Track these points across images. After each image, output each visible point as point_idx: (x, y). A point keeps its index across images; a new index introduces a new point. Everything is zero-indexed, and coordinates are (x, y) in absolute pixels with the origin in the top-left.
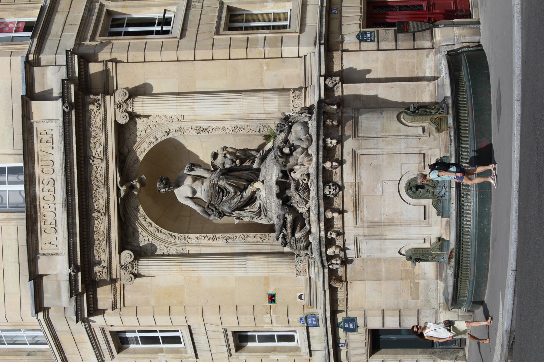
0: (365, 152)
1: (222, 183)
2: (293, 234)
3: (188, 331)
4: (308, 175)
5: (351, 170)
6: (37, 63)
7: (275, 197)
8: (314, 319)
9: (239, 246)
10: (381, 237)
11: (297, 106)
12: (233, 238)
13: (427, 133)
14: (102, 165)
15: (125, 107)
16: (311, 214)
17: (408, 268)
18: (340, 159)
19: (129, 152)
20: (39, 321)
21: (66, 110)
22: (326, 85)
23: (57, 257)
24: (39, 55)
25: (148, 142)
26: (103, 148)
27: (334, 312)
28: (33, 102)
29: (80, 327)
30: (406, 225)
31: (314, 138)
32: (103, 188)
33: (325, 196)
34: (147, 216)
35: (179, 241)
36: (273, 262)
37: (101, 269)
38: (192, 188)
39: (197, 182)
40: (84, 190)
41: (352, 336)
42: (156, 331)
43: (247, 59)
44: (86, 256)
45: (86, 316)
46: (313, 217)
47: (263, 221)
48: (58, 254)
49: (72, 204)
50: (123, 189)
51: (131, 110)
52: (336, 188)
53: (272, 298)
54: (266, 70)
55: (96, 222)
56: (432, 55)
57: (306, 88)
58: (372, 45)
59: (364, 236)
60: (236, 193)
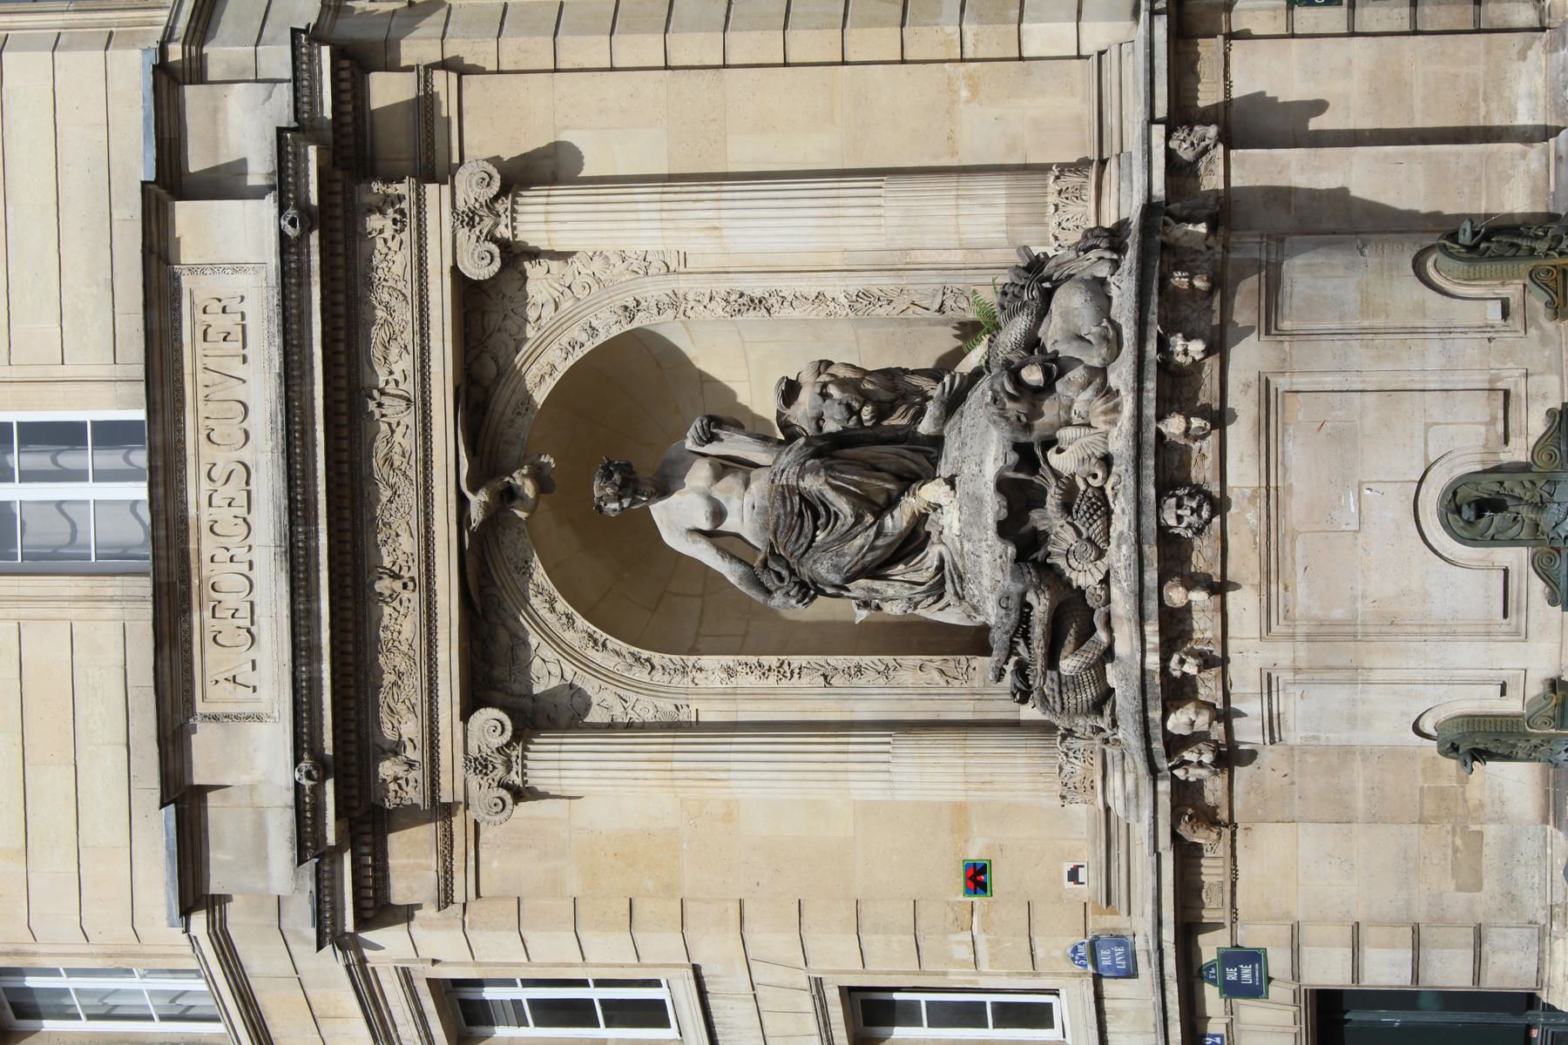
0: (1301, 382)
1: (813, 484)
2: (1052, 661)
3: (693, 983)
4: (1107, 461)
5: (1252, 444)
6: (196, 72)
7: (991, 533)
8: (1119, 951)
9: (867, 697)
10: (1354, 675)
11: (1070, 225)
12: (847, 672)
13: (1516, 321)
14: (409, 418)
15: (488, 222)
16: (1115, 592)
17: (1445, 783)
18: (1216, 406)
19: (500, 375)
20: (193, 940)
21: (291, 232)
22: (1170, 154)
23: (255, 726)
24: (201, 44)
25: (564, 341)
26: (412, 359)
27: (1189, 928)
28: (178, 203)
29: (331, 963)
30: (1441, 634)
31: (1128, 333)
32: (410, 496)
33: (1163, 531)
34: (557, 594)
35: (667, 678)
36: (983, 756)
37: (400, 770)
38: (710, 499)
39: (730, 481)
40: (346, 502)
41: (1249, 1010)
42: (583, 983)
43: (903, 61)
44: (352, 726)
45: (349, 926)
46: (1122, 605)
47: (953, 616)
48: (259, 718)
49: (306, 549)
50: (478, 502)
51: (507, 234)
52: (1200, 506)
53: (977, 878)
54: (968, 101)
55: (387, 610)
56: (1537, 53)
57: (1103, 163)
59: (1297, 670)
60: (859, 519)
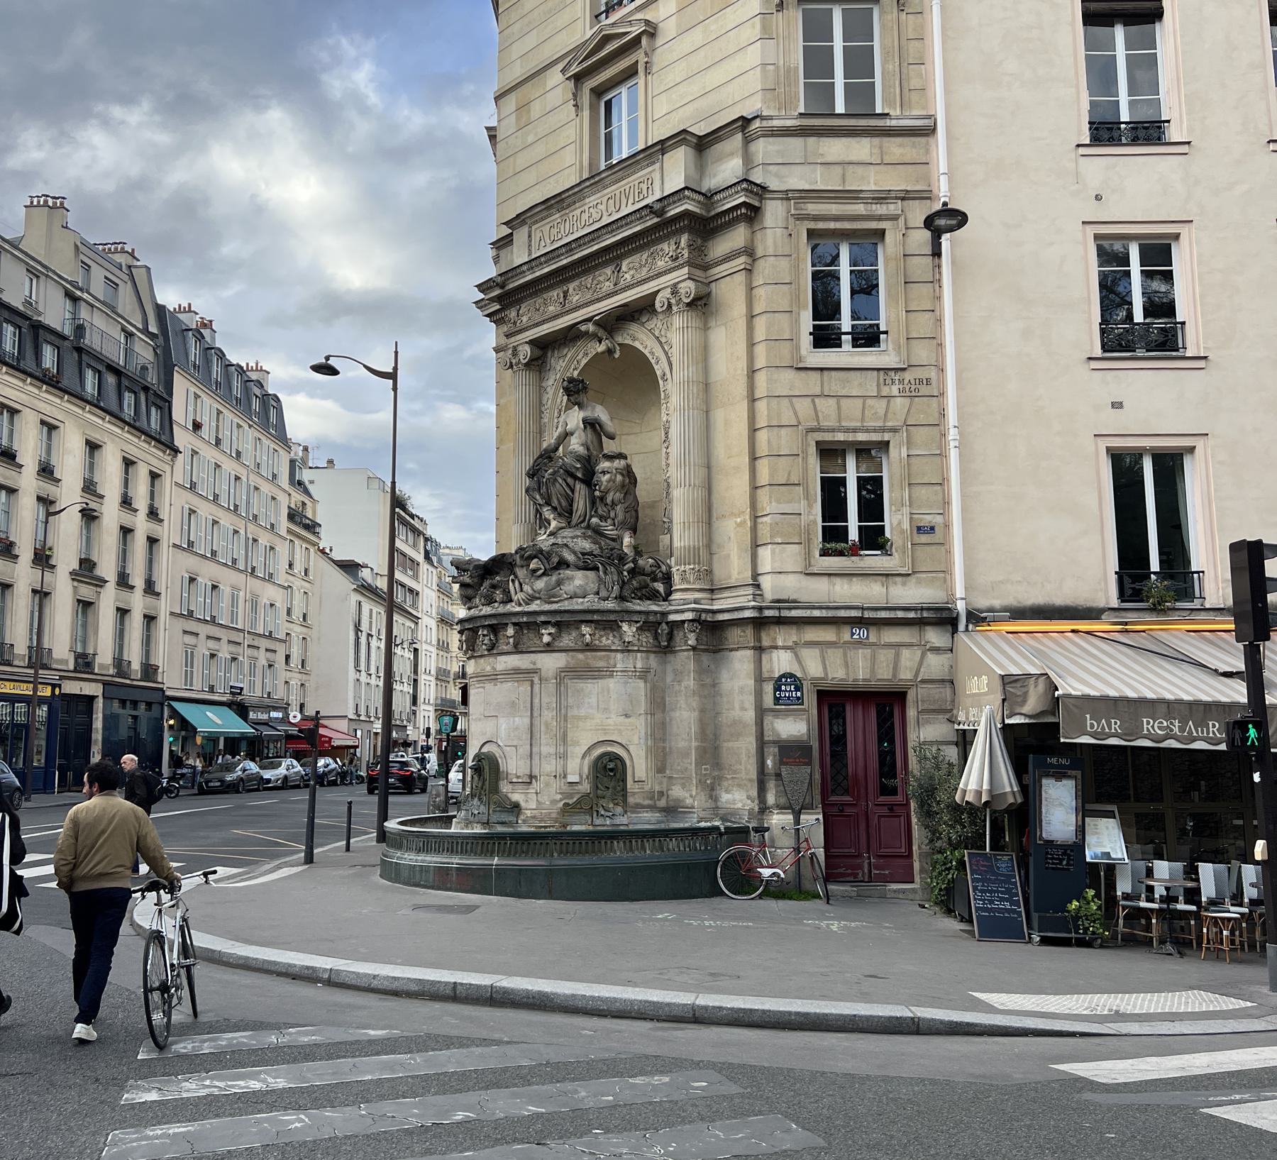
0: (536, 688)
13: (565, 788)
50: (591, 327)
57: (712, 591)
58: (768, 700)
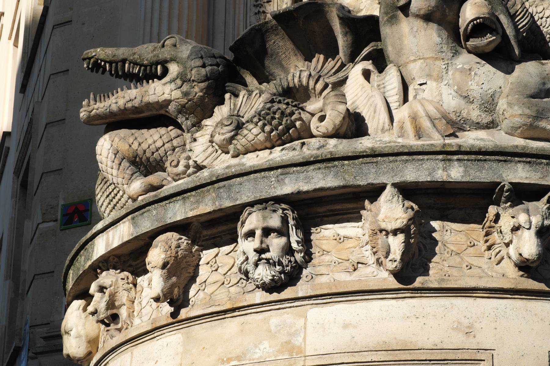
5: (371, 343)
